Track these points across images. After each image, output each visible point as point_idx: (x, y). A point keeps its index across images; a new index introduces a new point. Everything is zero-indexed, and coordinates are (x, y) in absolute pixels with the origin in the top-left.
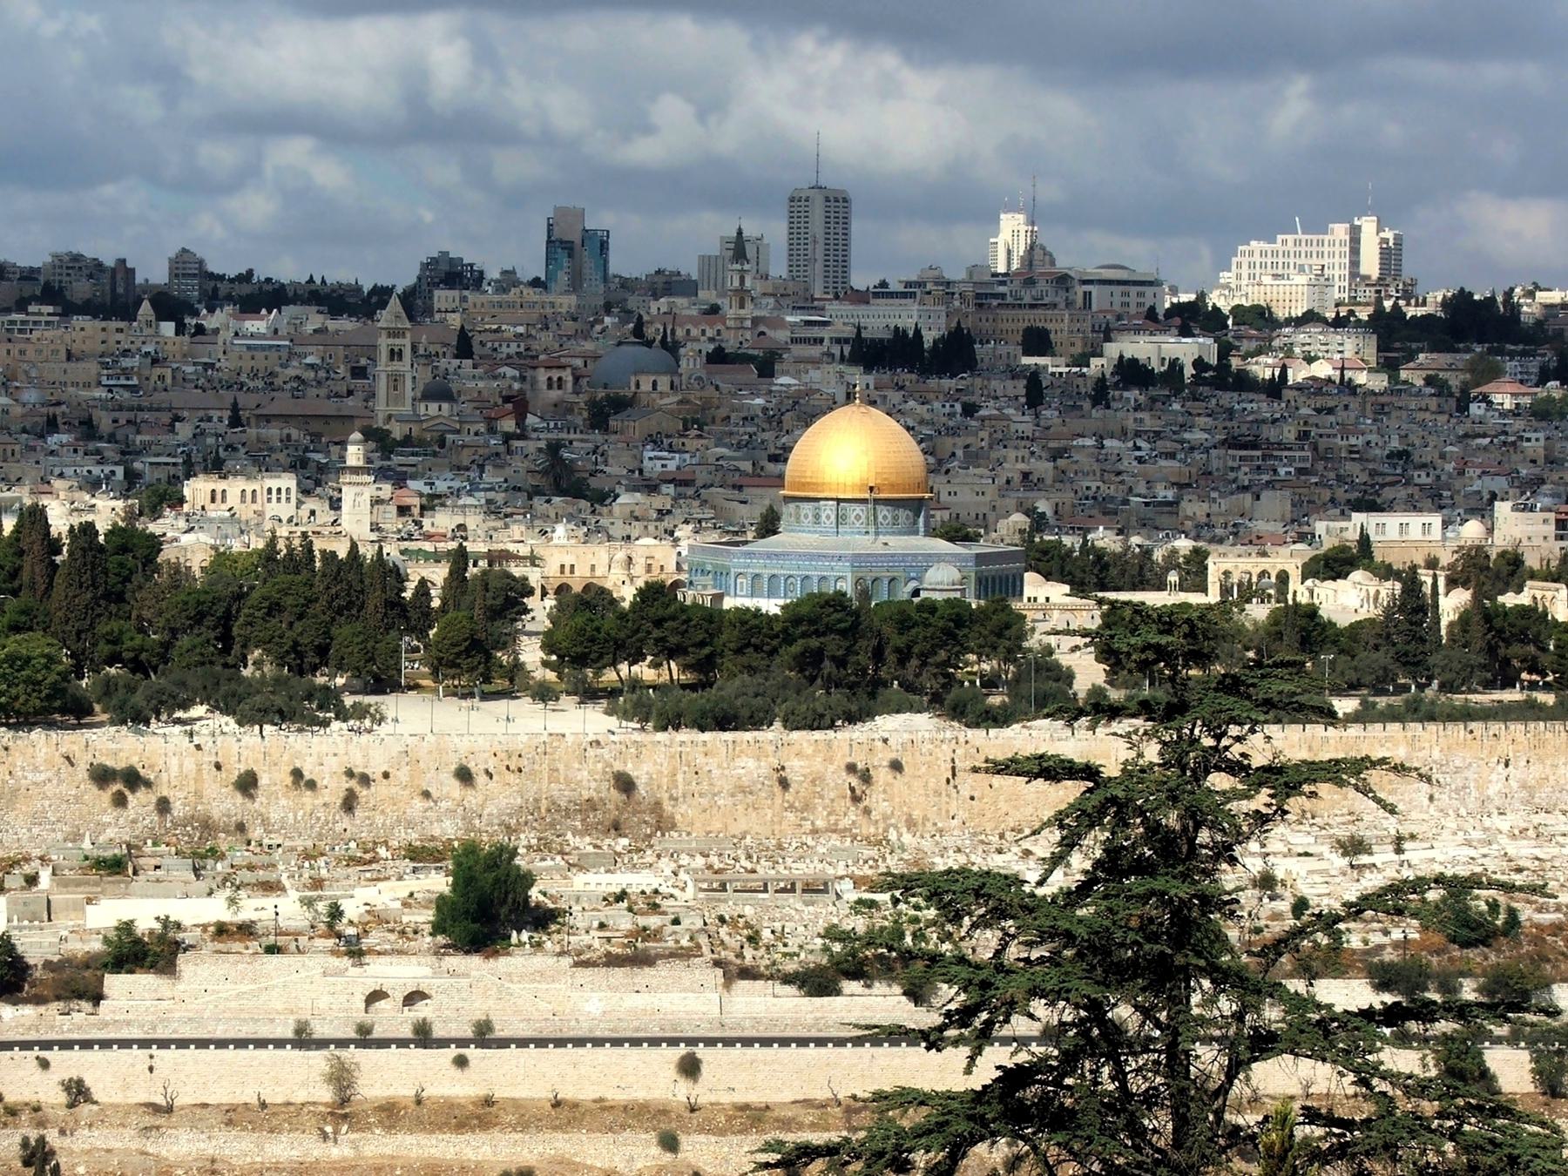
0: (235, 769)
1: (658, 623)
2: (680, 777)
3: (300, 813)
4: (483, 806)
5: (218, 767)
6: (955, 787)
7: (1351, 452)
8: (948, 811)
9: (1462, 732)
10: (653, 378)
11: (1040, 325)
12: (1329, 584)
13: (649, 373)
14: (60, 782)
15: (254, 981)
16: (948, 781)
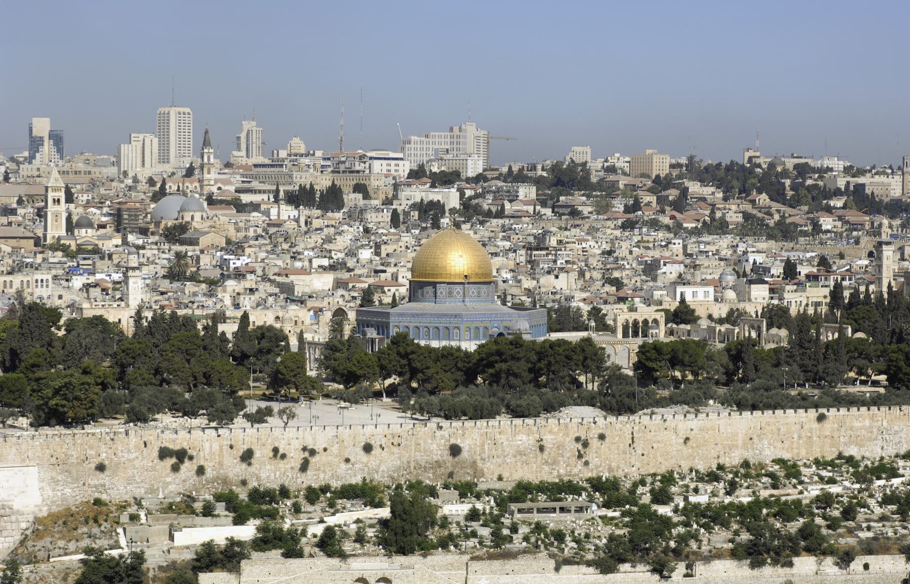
0: (242, 448)
1: (405, 356)
2: (486, 447)
3: (278, 473)
4: (379, 466)
5: (231, 447)
6: (634, 448)
7: (583, 251)
8: (630, 463)
9: (898, 411)
10: (191, 214)
11: (362, 182)
12: (682, 326)
13: (189, 211)
14: (143, 459)
15: (287, 574)
16: (630, 445)
